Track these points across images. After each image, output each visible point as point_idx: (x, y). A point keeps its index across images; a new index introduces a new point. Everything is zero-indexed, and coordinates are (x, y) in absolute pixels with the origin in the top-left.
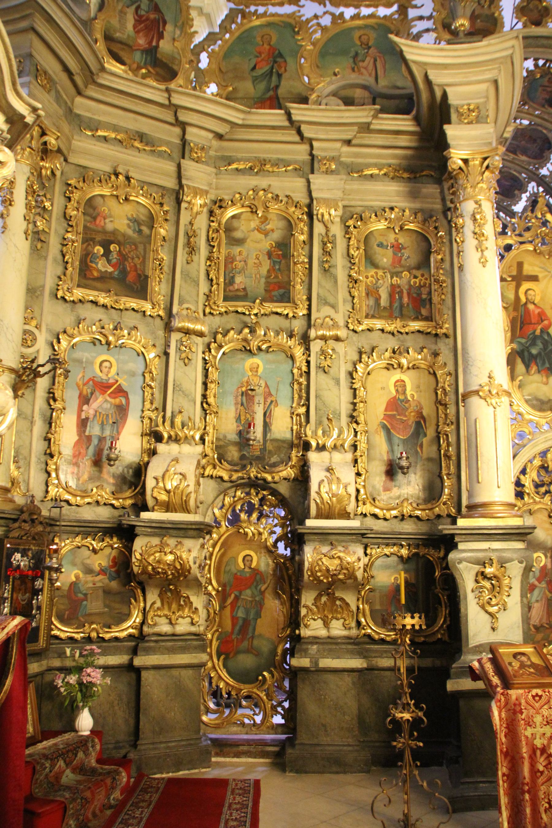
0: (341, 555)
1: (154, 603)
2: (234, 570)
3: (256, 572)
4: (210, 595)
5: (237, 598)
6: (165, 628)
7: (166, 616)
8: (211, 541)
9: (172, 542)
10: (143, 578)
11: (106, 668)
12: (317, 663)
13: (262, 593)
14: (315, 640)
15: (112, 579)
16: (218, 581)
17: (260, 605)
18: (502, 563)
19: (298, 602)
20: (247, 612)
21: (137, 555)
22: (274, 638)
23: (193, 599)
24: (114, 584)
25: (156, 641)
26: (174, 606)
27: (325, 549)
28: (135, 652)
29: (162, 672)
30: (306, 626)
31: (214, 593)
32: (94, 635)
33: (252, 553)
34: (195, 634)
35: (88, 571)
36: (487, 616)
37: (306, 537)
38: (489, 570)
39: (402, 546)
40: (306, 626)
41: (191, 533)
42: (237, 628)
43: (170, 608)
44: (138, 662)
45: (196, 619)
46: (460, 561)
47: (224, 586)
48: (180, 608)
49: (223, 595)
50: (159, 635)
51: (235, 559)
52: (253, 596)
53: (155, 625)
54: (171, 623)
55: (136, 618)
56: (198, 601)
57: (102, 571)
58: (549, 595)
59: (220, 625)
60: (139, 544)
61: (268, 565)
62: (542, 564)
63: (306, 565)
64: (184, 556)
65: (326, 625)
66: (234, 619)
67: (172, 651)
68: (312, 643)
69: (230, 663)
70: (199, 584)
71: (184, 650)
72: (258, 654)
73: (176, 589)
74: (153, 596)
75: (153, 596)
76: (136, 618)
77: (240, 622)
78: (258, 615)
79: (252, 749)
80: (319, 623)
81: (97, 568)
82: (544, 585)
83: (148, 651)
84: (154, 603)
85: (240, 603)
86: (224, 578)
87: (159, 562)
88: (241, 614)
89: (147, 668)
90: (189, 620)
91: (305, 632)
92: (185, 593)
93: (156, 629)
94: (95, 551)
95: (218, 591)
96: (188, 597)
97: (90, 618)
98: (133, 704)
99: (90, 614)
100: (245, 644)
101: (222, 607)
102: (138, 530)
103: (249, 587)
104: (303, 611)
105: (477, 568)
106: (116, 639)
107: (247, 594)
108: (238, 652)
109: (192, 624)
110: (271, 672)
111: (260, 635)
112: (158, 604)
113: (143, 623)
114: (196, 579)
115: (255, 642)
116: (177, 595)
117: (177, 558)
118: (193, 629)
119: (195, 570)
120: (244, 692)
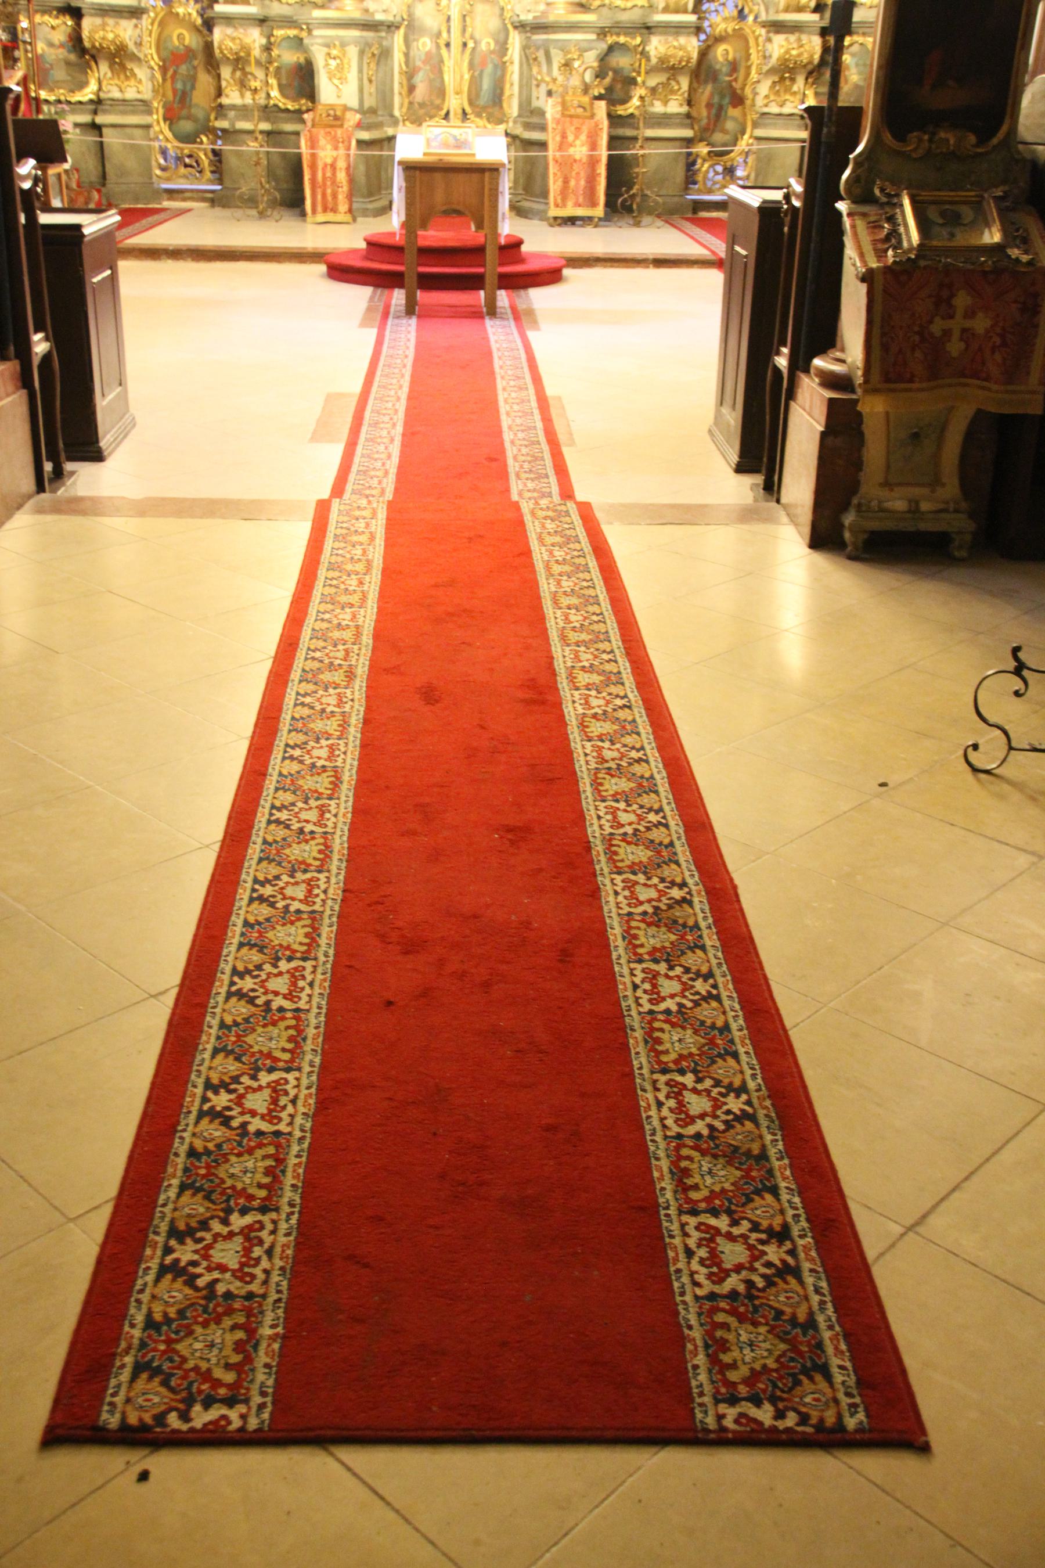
0: (241, 36)
1: (105, 74)
2: (171, 48)
3: (188, 49)
4: (152, 68)
5: (175, 72)
6: (116, 94)
7: (117, 85)
8: (150, 20)
9: (111, 21)
10: (94, 52)
11: (76, 125)
12: (233, 125)
13: (195, 68)
14: (233, 107)
15: (69, 52)
16: (160, 58)
17: (193, 79)
18: (343, 45)
19: (219, 76)
20: (184, 84)
21: (85, 34)
22: (207, 107)
23: (137, 71)
24: (73, 57)
25: (111, 105)
26: (122, 77)
27: (230, 31)
28: (95, 112)
29: (119, 129)
30: (227, 96)
31: (156, 68)
32: (62, 98)
33: (185, 32)
34: (141, 101)
35: (51, 45)
36: (334, 88)
37: (216, 21)
38: (334, 52)
39: (302, 29)
40: (227, 96)
41: (125, 14)
42: (178, 98)
43: (119, 79)
44: (99, 120)
45: (141, 88)
46: (312, 45)
47: (164, 61)
48: (127, 78)
49: (164, 70)
50: (113, 100)
51: (171, 37)
52: (188, 69)
53: (109, 92)
54: (121, 91)
55: (93, 86)
56: (141, 73)
57: (62, 46)
58: (432, 76)
59: (164, 95)
60: (87, 23)
61: (198, 42)
62: (427, 49)
63: (216, 44)
64: (122, 34)
65: (242, 96)
66: (175, 91)
67: (124, 113)
68: (231, 110)
69: (174, 127)
70: (139, 59)
71: (134, 112)
72: (195, 120)
73: (121, 61)
74: (104, 67)
75: (104, 67)
76: (93, 86)
77: (179, 93)
78: (193, 87)
79: (195, 195)
80: (237, 93)
81: (57, 43)
82: (428, 68)
83: (105, 112)
84: (105, 74)
85: (178, 76)
86: (164, 54)
87: (103, 38)
88: (179, 86)
89: (106, 126)
90: (135, 89)
91: (224, 101)
92: (129, 65)
93: (110, 95)
94: (53, 28)
95: (159, 66)
96: (132, 70)
97: (58, 85)
98: (99, 155)
99: (58, 82)
100: (184, 112)
101: (164, 80)
102: (84, 11)
103: (185, 62)
104: (224, 84)
105: (326, 50)
106: (80, 103)
107: (183, 69)
108: (179, 119)
109: (139, 92)
110: (207, 136)
111: (197, 105)
112: (109, 74)
113: (100, 89)
114: (134, 54)
115: (193, 111)
116: (123, 67)
117: (117, 36)
118: (139, 96)
119: (132, 47)
120: (186, 152)
